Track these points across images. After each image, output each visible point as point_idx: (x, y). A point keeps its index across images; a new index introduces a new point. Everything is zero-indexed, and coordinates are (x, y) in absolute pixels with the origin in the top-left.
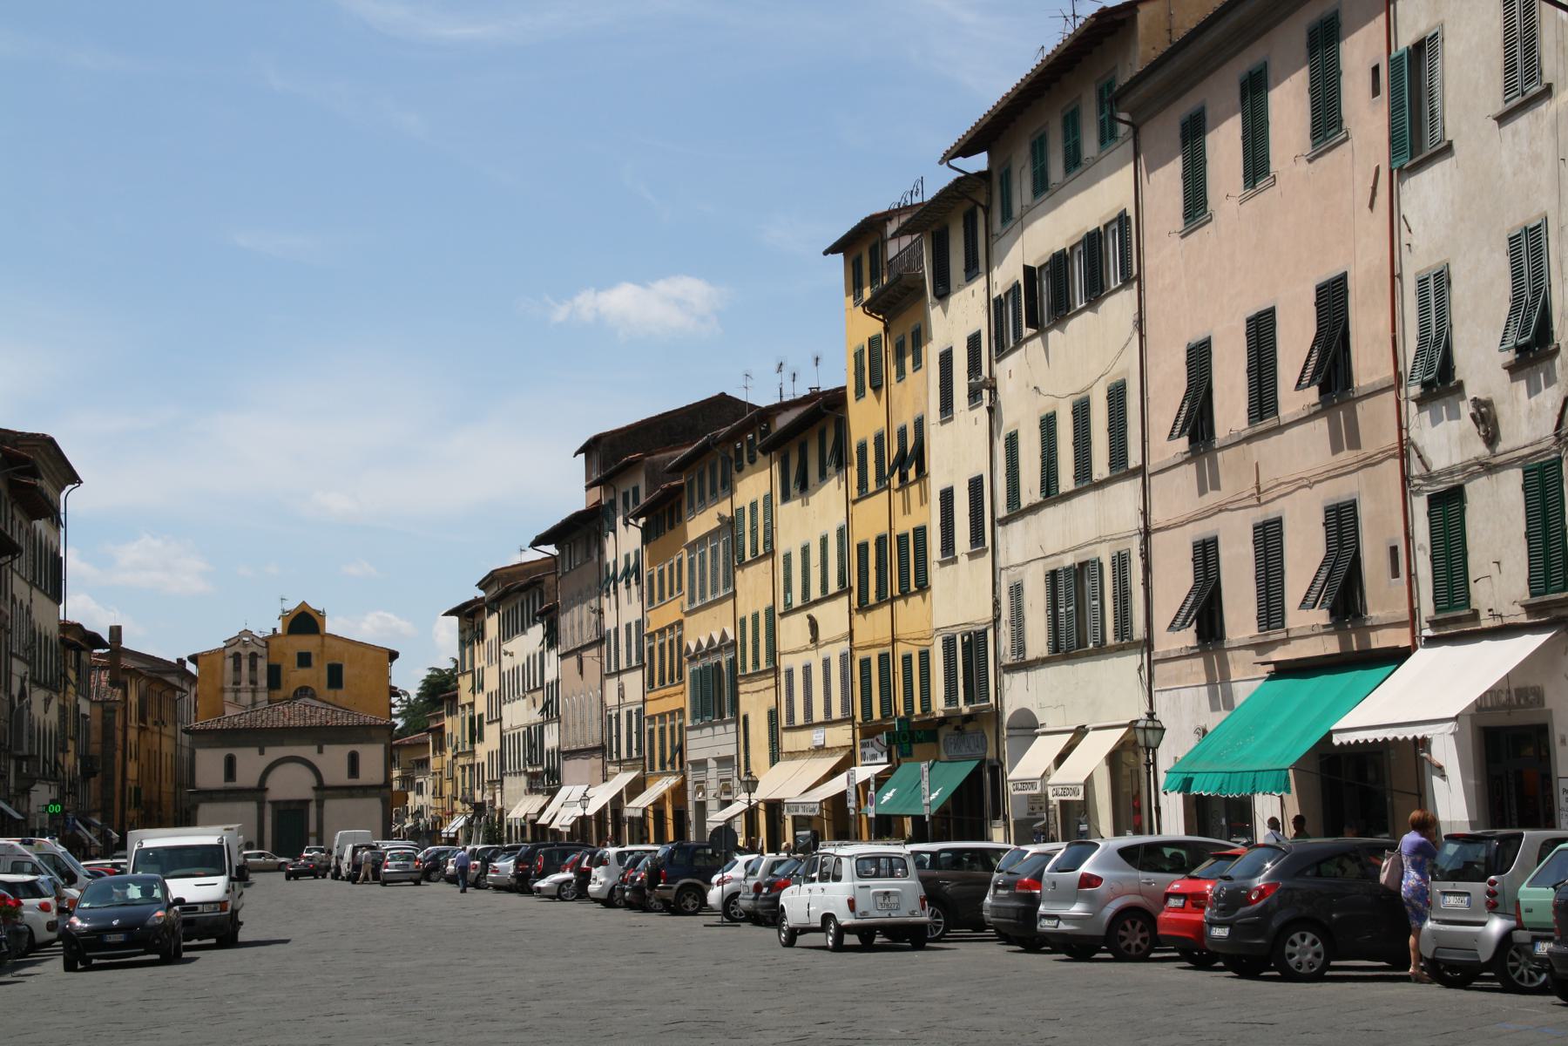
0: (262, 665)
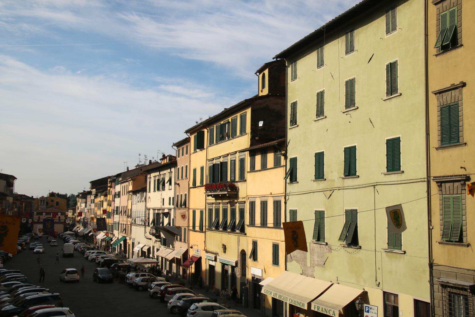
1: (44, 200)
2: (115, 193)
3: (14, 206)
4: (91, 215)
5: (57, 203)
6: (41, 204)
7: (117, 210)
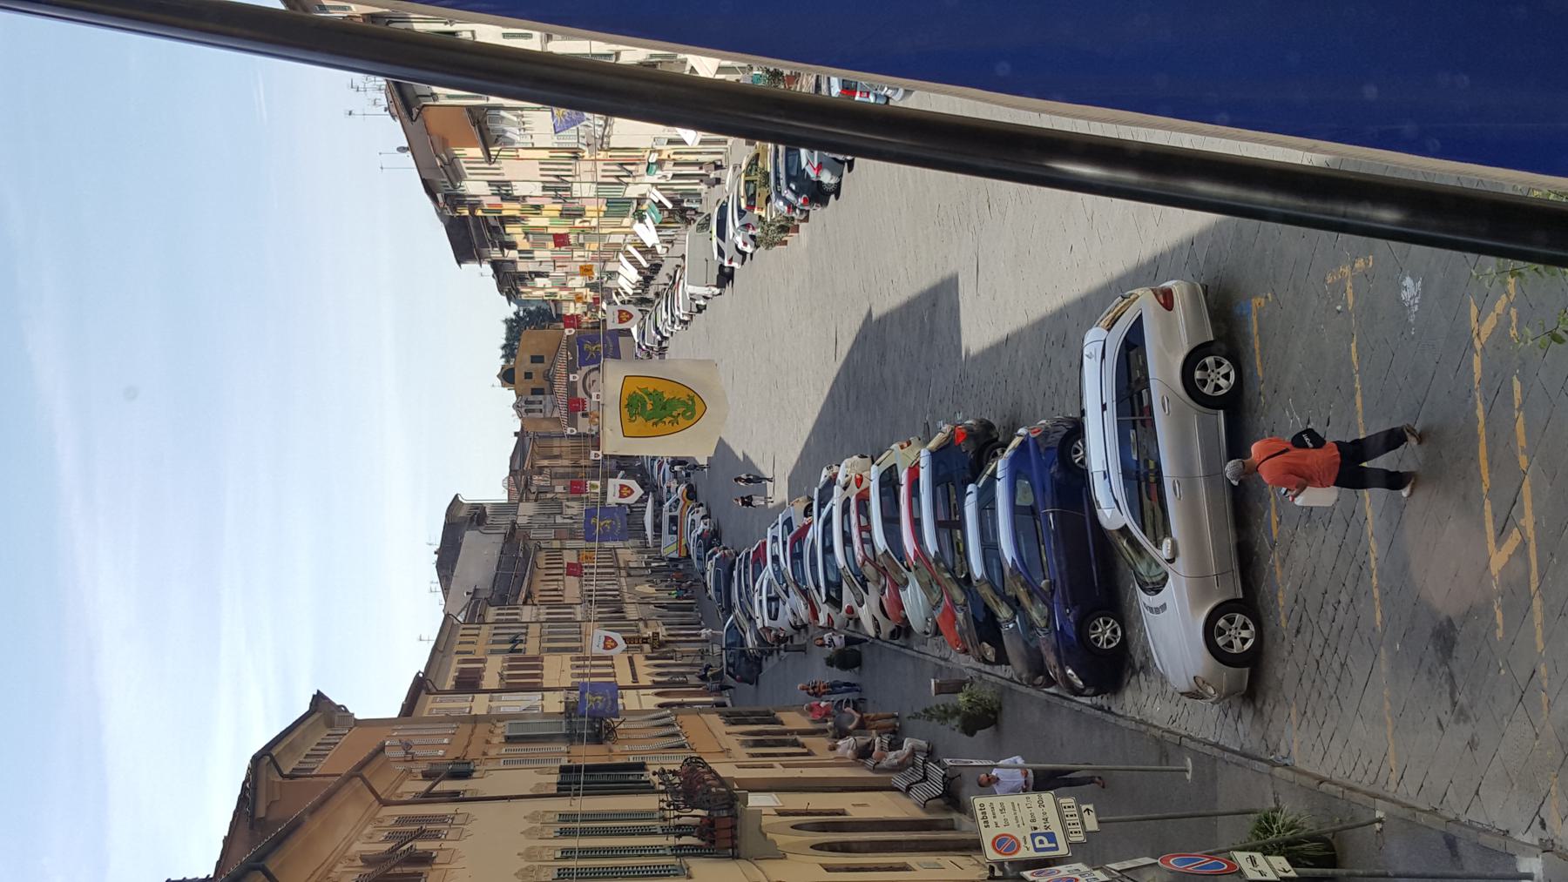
0: (531, 398)
1: (527, 402)
2: (493, 194)
3: (549, 496)
4: (574, 259)
5: (536, 359)
6: (541, 411)
7: (556, 189)
